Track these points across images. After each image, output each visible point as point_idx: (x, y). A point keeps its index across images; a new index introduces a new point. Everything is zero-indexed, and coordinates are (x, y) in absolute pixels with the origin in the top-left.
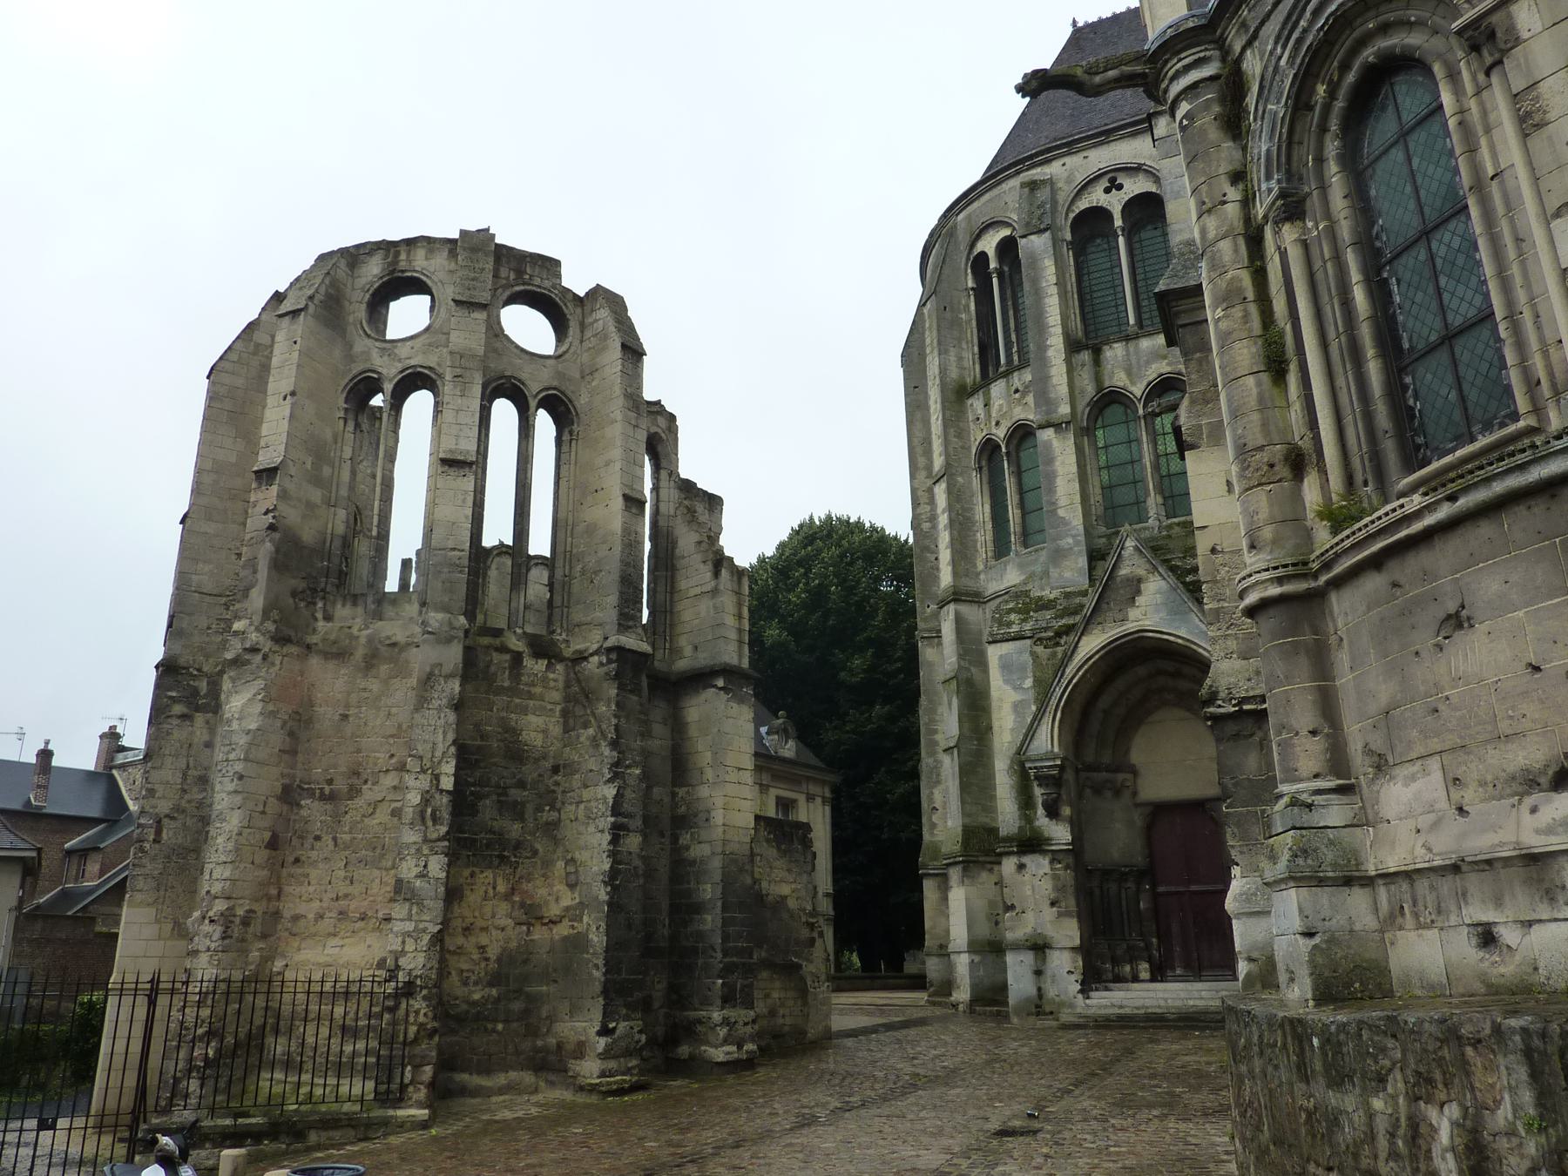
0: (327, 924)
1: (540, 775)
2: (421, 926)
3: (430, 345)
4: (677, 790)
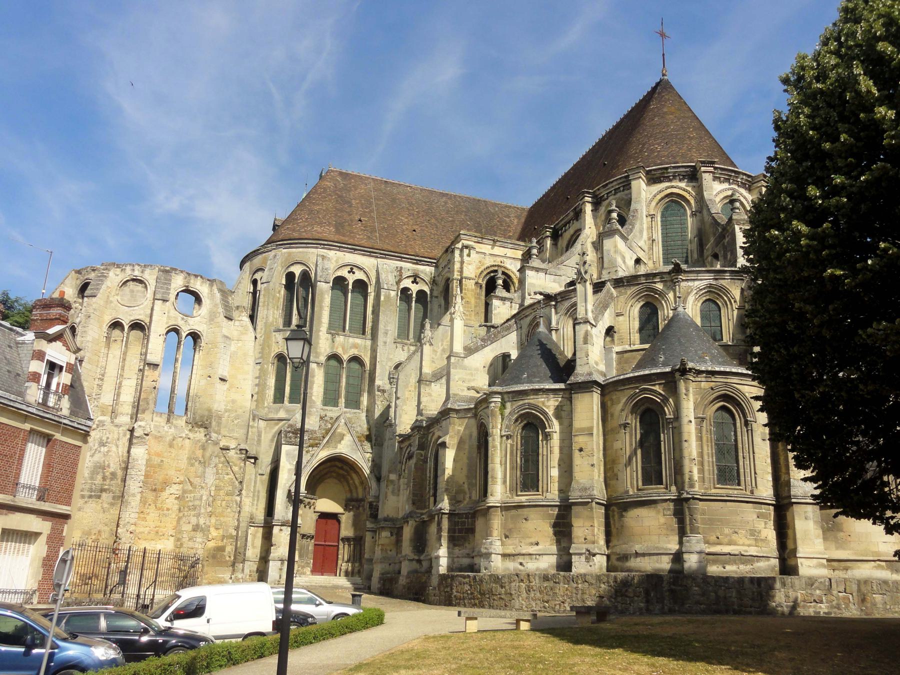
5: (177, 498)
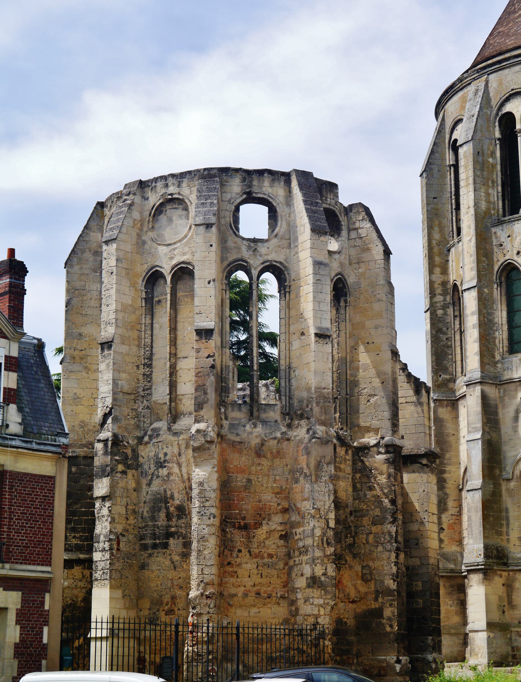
0: (251, 599)
1: (346, 517)
2: (326, 601)
3: (279, 246)
5: (281, 537)
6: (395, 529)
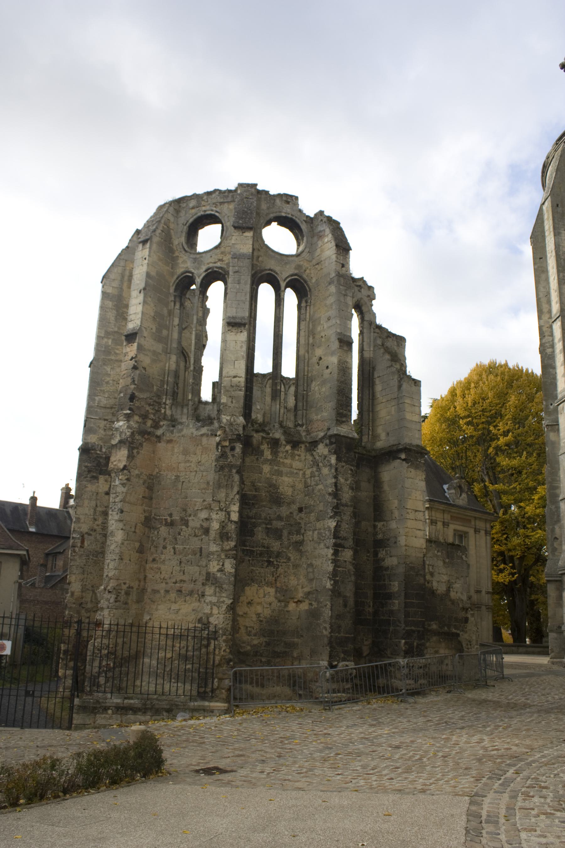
2: (221, 600)
4: (377, 523)
6: (335, 524)
